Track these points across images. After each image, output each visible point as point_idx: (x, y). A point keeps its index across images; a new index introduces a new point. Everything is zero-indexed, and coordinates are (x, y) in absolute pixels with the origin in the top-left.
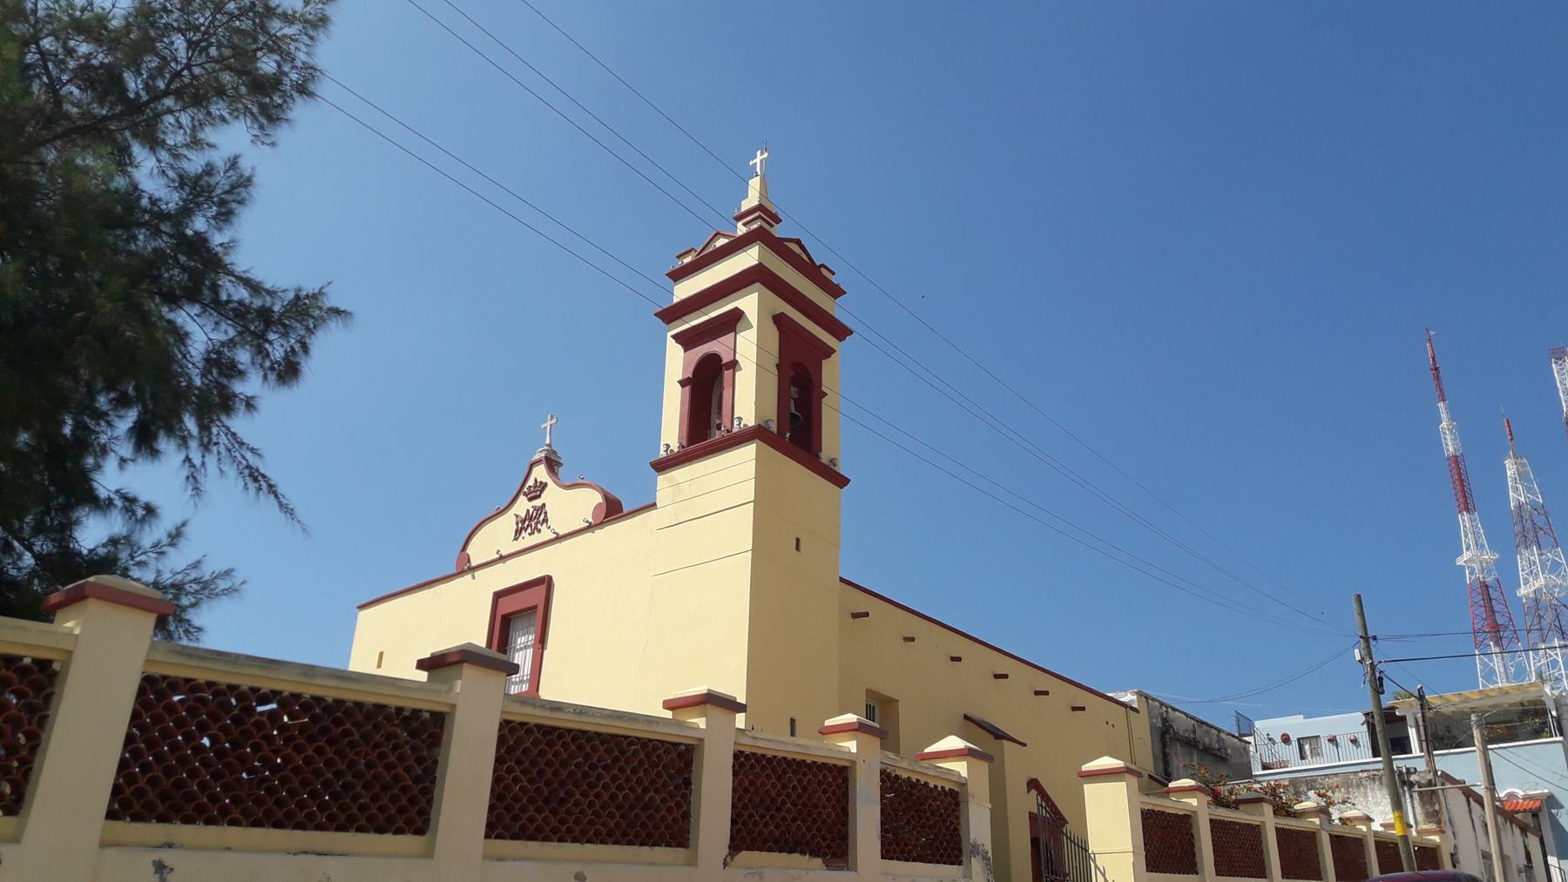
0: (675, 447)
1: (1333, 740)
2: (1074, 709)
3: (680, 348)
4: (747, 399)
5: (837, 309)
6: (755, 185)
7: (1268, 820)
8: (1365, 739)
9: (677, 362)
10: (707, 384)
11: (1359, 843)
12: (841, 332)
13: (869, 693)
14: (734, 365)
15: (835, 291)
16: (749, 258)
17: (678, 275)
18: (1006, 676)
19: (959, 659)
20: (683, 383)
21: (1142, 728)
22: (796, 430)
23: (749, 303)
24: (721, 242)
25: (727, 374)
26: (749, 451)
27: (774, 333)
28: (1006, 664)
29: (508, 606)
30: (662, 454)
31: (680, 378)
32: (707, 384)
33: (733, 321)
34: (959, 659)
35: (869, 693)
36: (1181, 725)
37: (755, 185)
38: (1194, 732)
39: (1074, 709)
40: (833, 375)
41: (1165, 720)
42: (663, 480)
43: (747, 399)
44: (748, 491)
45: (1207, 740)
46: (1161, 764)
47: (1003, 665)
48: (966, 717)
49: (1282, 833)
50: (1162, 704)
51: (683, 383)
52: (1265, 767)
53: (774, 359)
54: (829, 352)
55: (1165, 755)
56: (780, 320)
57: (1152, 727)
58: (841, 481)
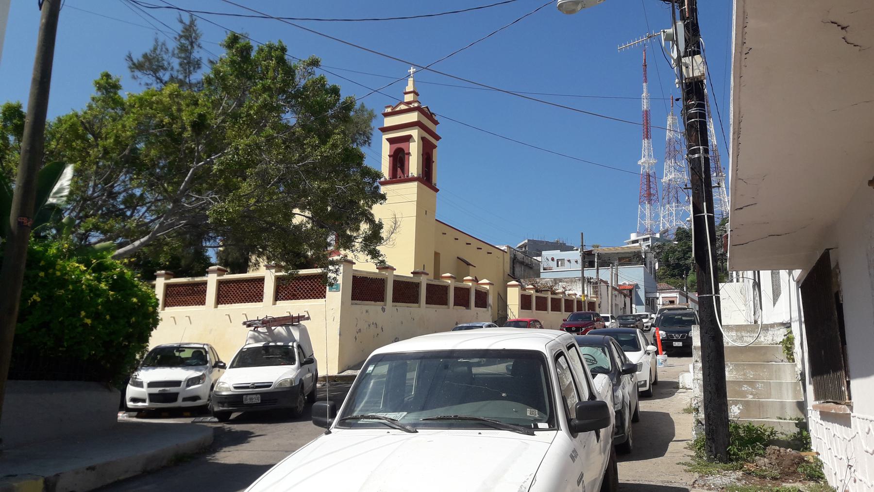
0: (388, 178)
1: (569, 261)
3: (388, 144)
4: (414, 166)
5: (437, 130)
6: (411, 81)
8: (580, 261)
11: (572, 301)
14: (409, 154)
16: (413, 117)
17: (387, 115)
23: (414, 133)
24: (403, 107)
26: (415, 184)
27: (421, 142)
28: (470, 240)
32: (399, 159)
33: (408, 138)
37: (411, 81)
40: (437, 155)
43: (414, 166)
47: (469, 240)
51: (390, 156)
53: (421, 152)
54: (435, 147)
56: (423, 139)
58: (437, 190)
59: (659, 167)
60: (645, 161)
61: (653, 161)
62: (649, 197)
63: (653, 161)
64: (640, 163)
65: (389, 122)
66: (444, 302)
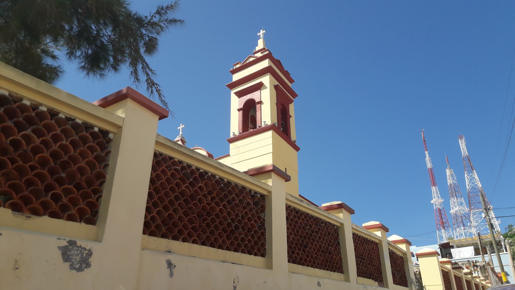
0: (237, 134)
4: (266, 115)
9: (236, 103)
10: (249, 111)
12: (295, 95)
14: (260, 103)
15: (292, 81)
16: (265, 64)
20: (239, 110)
22: (282, 127)
23: (266, 80)
24: (252, 59)
25: (258, 106)
26: (270, 133)
30: (232, 136)
31: (238, 108)
32: (249, 111)
33: (259, 87)
42: (232, 146)
43: (266, 115)
44: (270, 149)
51: (239, 110)
54: (291, 102)
56: (276, 87)
59: (447, 205)
60: (436, 201)
61: (441, 200)
62: (443, 225)
63: (441, 200)
64: (432, 202)
65: (236, 77)
66: (334, 263)
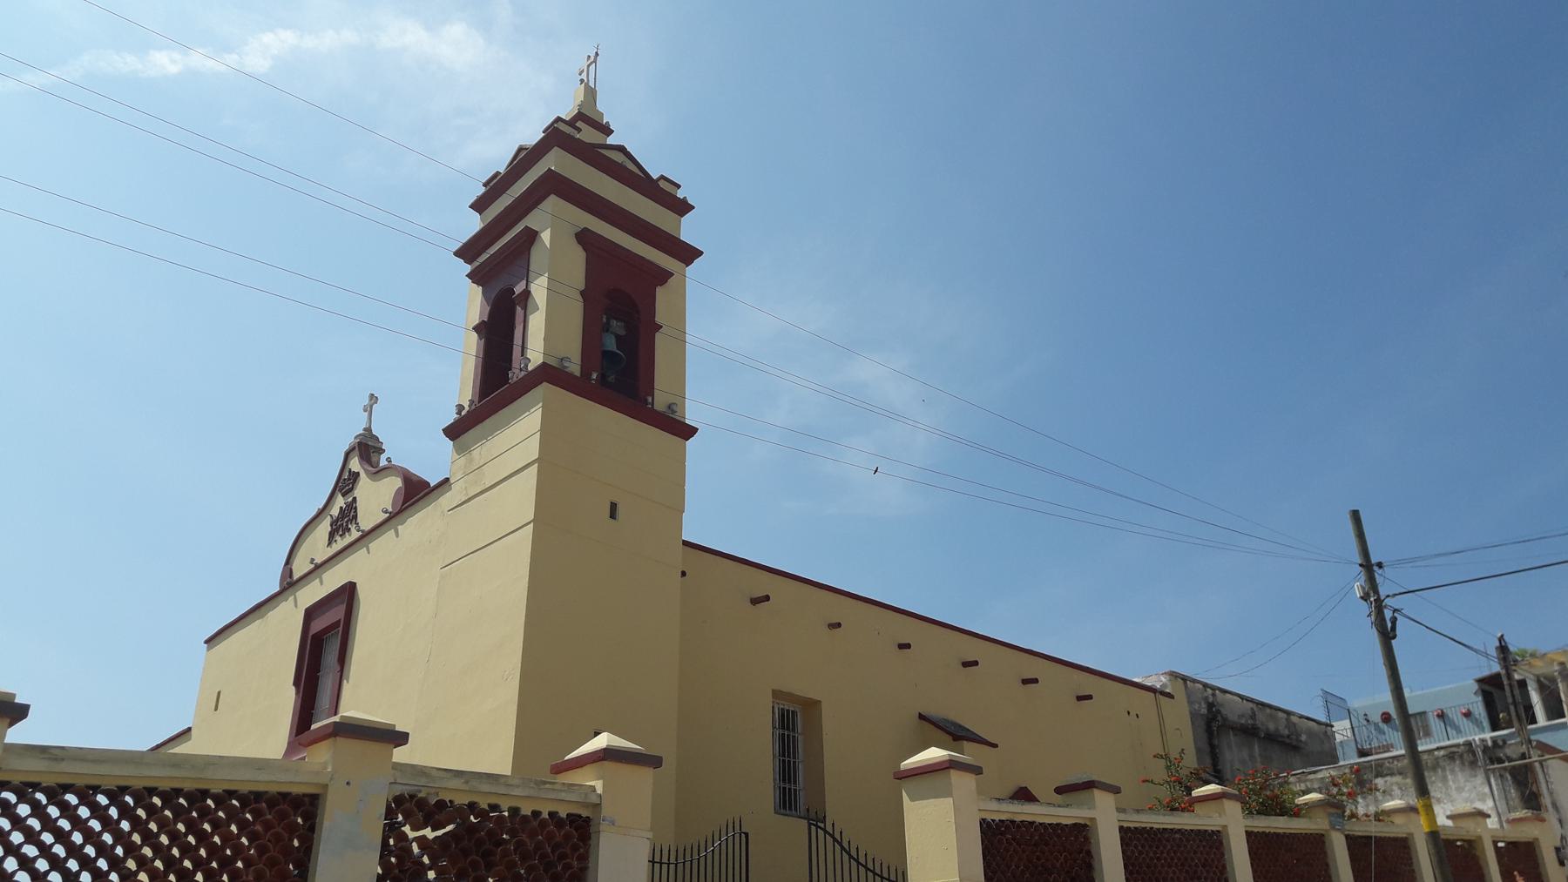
2: (1080, 698)
7: (1234, 824)
13: (776, 694)
18: (975, 663)
19: (908, 646)
21: (1179, 717)
29: (318, 626)
34: (908, 646)
35: (776, 694)
36: (1234, 712)
38: (1253, 716)
39: (1080, 698)
41: (1210, 706)
45: (1272, 727)
46: (1208, 761)
48: (921, 717)
49: (1256, 841)
50: (1206, 686)
52: (1362, 753)
55: (1212, 747)
57: (1194, 716)
